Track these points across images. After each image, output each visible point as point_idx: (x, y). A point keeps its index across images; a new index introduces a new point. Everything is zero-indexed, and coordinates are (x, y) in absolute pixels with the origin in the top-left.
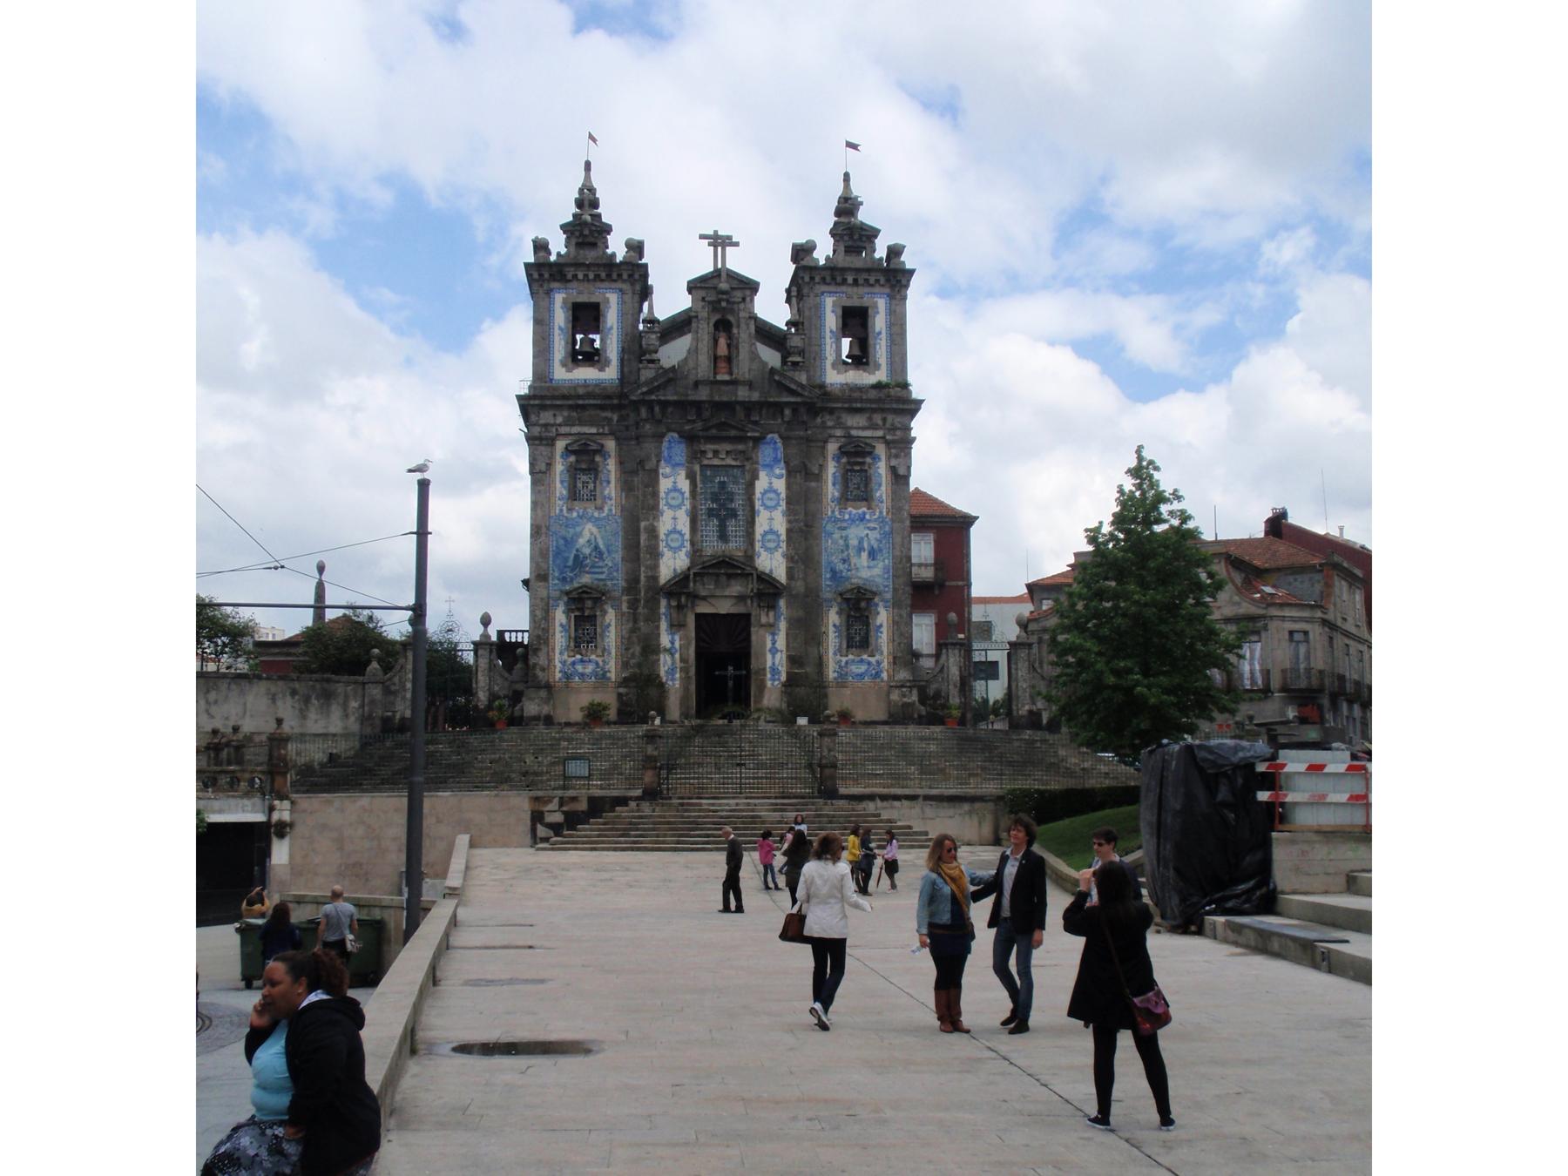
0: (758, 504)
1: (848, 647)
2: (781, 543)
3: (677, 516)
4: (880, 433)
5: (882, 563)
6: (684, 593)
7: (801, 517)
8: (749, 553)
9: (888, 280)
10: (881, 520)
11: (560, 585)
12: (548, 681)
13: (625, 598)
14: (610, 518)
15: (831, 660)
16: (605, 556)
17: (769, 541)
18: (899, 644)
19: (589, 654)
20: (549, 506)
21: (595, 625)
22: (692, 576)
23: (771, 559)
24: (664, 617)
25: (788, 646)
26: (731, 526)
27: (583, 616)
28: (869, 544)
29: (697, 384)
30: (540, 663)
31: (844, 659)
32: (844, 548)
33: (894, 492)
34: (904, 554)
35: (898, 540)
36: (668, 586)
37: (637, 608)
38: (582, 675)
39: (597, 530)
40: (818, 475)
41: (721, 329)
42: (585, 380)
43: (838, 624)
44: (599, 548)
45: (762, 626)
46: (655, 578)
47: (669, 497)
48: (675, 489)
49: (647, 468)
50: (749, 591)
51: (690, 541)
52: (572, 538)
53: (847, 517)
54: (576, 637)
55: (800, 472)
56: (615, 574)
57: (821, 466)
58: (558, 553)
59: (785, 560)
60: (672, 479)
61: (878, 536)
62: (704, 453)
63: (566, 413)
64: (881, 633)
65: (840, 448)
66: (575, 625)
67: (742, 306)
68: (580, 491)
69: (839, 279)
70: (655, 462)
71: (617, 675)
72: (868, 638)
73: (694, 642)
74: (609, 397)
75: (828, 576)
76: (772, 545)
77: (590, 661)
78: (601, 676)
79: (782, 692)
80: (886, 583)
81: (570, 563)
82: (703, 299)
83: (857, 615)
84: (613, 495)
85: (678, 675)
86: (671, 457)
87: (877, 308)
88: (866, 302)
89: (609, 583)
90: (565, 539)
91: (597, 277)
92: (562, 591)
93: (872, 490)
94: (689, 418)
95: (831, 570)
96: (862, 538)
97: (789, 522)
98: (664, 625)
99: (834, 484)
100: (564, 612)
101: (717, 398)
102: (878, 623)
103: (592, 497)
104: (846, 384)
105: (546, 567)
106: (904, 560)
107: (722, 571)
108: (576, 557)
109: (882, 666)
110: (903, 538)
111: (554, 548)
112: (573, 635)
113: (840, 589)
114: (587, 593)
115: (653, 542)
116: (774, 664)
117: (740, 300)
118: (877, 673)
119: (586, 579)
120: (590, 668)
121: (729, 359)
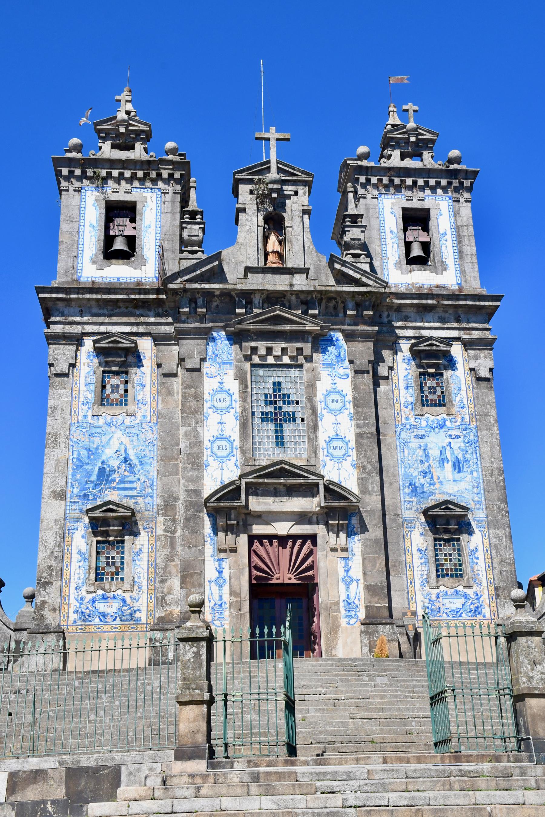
0: (320, 407)
1: (438, 576)
2: (350, 451)
3: (224, 420)
4: (454, 334)
5: (469, 476)
6: (235, 508)
7: (373, 420)
8: (313, 462)
9: (450, 183)
10: (464, 427)
11: (81, 502)
12: (59, 626)
13: (160, 519)
14: (144, 425)
15: (418, 593)
16: (136, 469)
17: (335, 448)
18: (501, 572)
19: (113, 589)
20: (71, 411)
21: (123, 553)
22: (243, 487)
23: (339, 469)
24: (209, 539)
25: (365, 574)
26: (288, 428)
27: (108, 542)
28: (452, 453)
29: (248, 270)
30: (50, 601)
31: (435, 591)
32: (423, 459)
33: (476, 397)
34: (495, 465)
35: (486, 449)
36: (214, 499)
37: (174, 532)
38: (104, 615)
39: (128, 439)
40: (387, 378)
41: (271, 226)
42: (118, 279)
43: (423, 549)
44: (131, 460)
45: (334, 550)
46: (197, 492)
47: (215, 399)
48: (221, 390)
49: (187, 367)
50: (314, 507)
51: (240, 448)
52: (97, 449)
53: (424, 424)
54: (97, 568)
55: (368, 372)
56: (148, 490)
57: (391, 368)
58: (80, 465)
59: (356, 470)
60: (218, 379)
61: (462, 445)
62: (254, 350)
63: (95, 310)
64: (477, 558)
65: (411, 349)
66: (98, 553)
67: (294, 198)
68: (108, 395)
69: (397, 181)
70: (198, 360)
71: (149, 614)
72: (460, 565)
73: (247, 569)
74: (147, 292)
75: (407, 491)
76: (340, 453)
77: (114, 598)
78: (129, 617)
79: (362, 632)
80: (476, 499)
81: (94, 478)
82: (251, 192)
83: (445, 537)
84: (148, 400)
85: (227, 613)
86: (217, 355)
87: (440, 210)
88: (426, 204)
89: (140, 500)
90: (90, 450)
91: (133, 177)
92: (81, 511)
93: (450, 395)
94: (237, 311)
95: (410, 484)
96: (444, 447)
97: (358, 426)
98: (209, 550)
99: (407, 388)
100: (83, 537)
101: (271, 287)
102: (472, 546)
103: (123, 402)
104: (413, 283)
105: (64, 483)
106: (496, 473)
107: (282, 481)
108: (102, 471)
109: (481, 599)
110: (492, 447)
111: (75, 460)
112: (93, 565)
113: (424, 506)
114: (110, 510)
115: (196, 450)
116: (348, 595)
117: (292, 193)
118: (477, 607)
119: (113, 496)
120: (114, 606)
121: (281, 257)
